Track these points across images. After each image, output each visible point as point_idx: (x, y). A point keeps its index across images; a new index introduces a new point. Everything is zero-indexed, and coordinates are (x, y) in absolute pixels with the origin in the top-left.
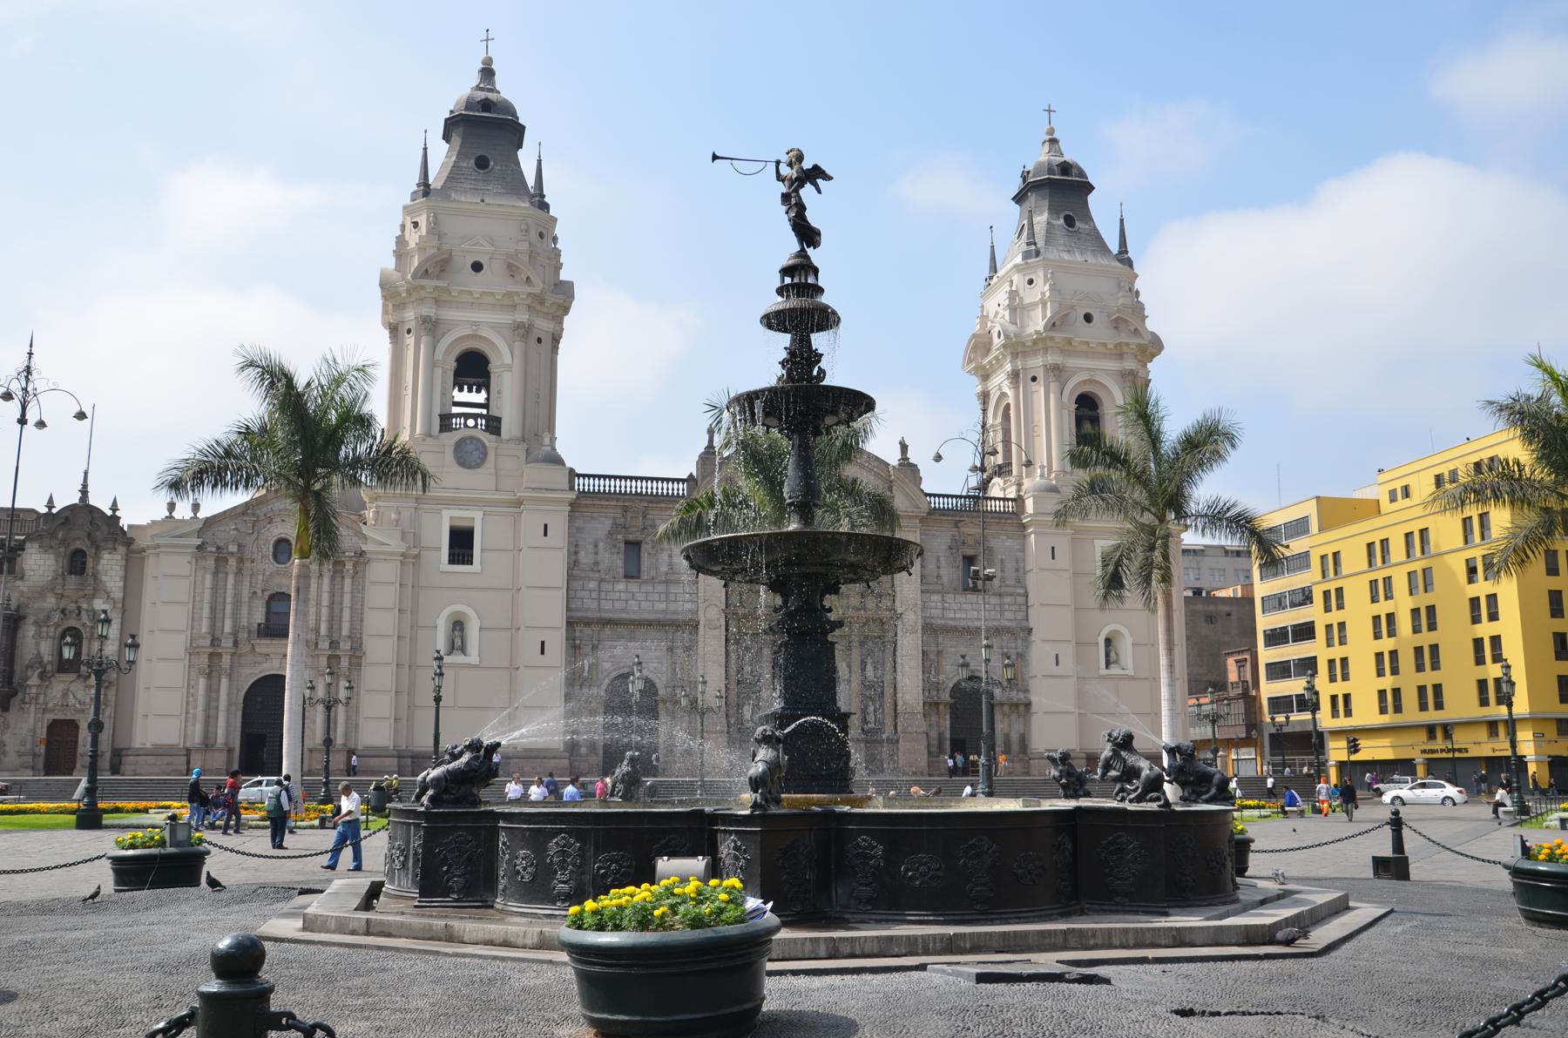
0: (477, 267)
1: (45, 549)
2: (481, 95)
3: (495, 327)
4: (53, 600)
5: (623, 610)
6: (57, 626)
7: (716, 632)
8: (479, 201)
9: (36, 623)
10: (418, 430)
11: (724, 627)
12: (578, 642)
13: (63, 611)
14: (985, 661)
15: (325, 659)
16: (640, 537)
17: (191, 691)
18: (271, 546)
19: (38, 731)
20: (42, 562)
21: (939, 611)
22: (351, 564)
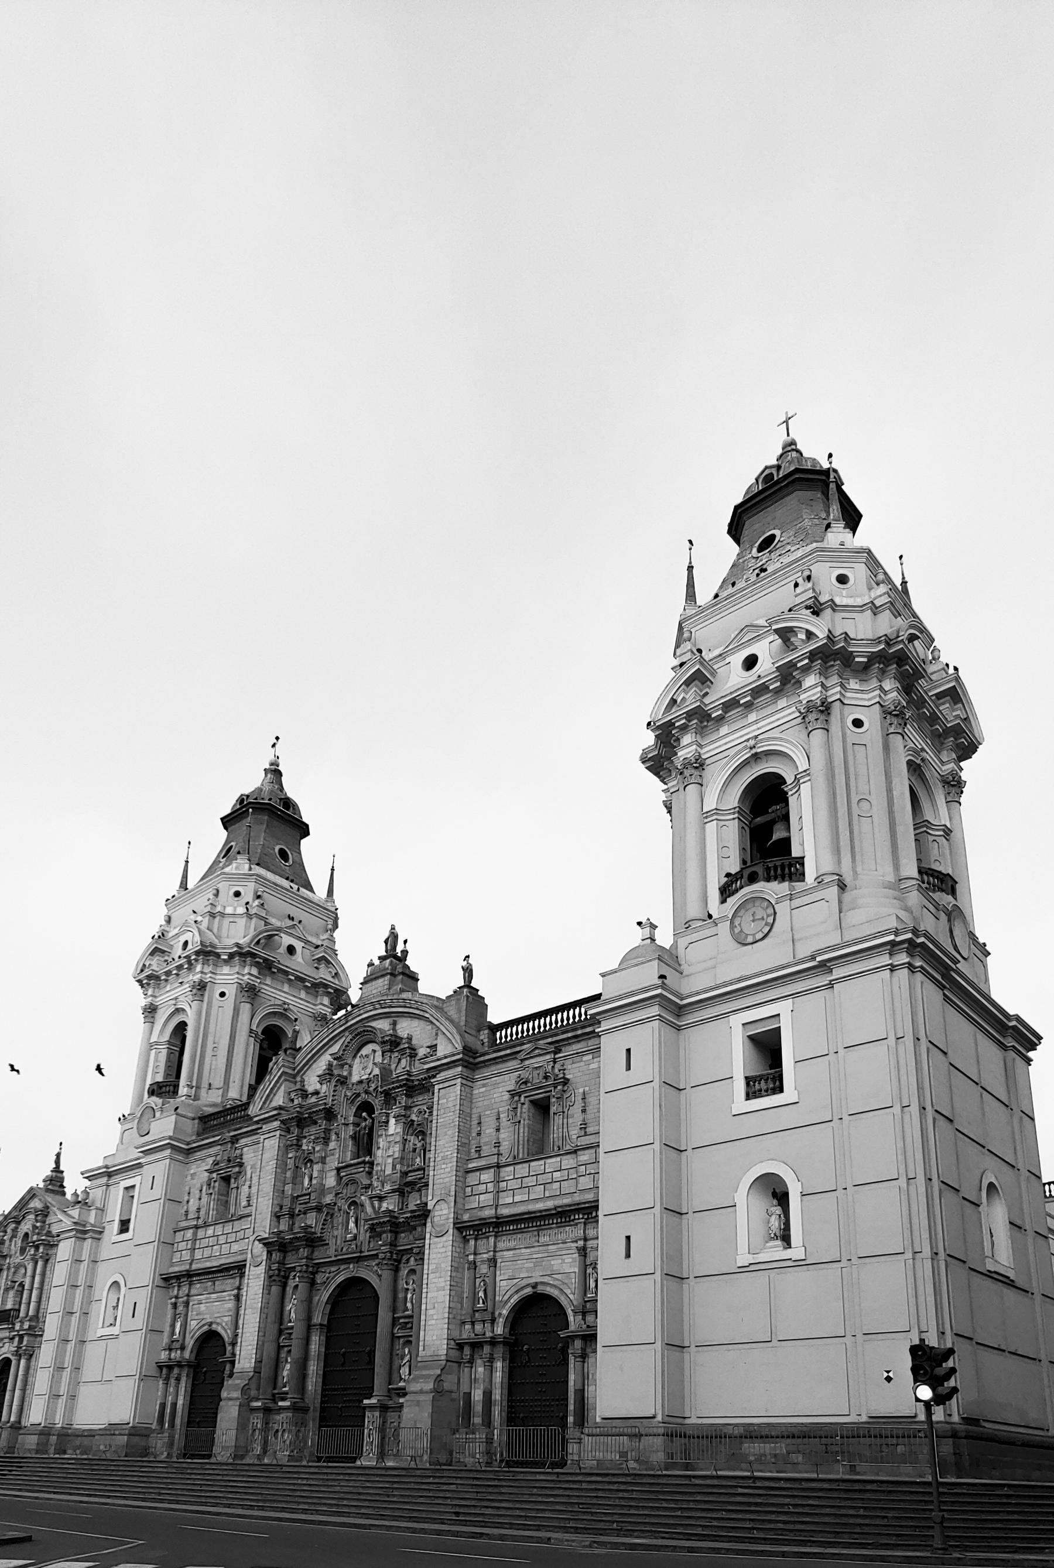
11: (264, 1263)
21: (491, 1196)
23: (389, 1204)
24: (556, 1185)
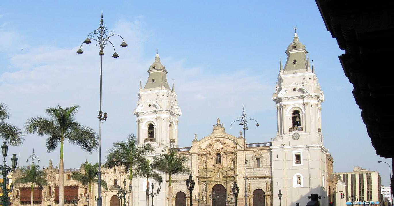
11: (198, 181)
14: (263, 185)
23: (228, 172)
24: (262, 173)
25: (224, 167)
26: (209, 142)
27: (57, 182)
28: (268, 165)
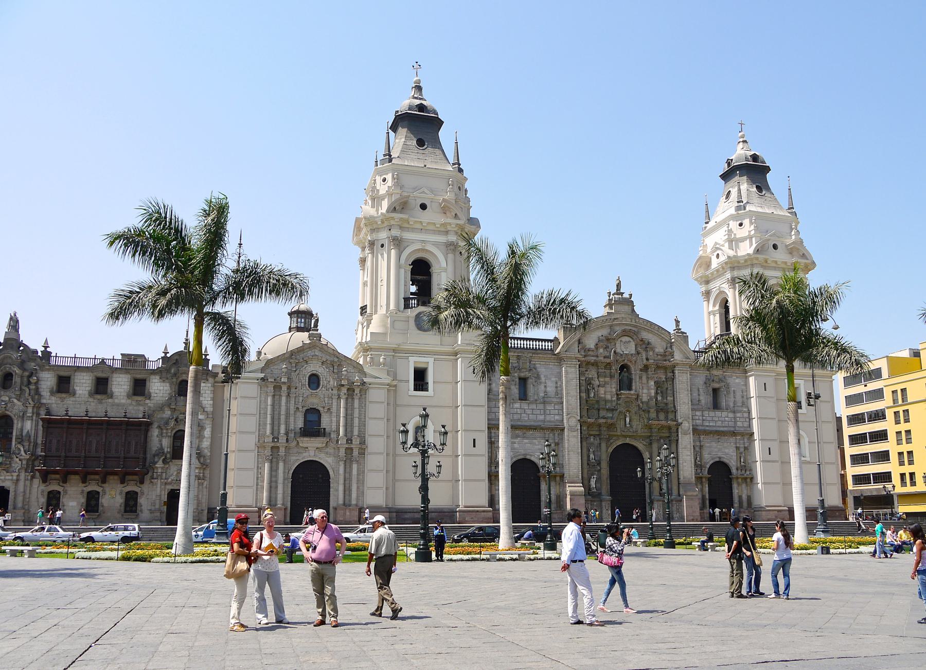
0: (423, 207)
1: (163, 379)
2: (418, 102)
3: (436, 244)
4: (169, 413)
5: (519, 420)
6: (173, 429)
7: (575, 434)
8: (423, 166)
9: (159, 427)
10: (392, 307)
11: (579, 431)
12: (493, 440)
13: (176, 420)
14: (726, 452)
15: (344, 450)
16: (527, 374)
17: (260, 470)
18: (307, 379)
19: (163, 496)
20: (162, 388)
21: (701, 421)
22: (359, 390)
24: (727, 422)
25: (641, 400)
26: (605, 332)
27: (44, 401)
28: (738, 404)
